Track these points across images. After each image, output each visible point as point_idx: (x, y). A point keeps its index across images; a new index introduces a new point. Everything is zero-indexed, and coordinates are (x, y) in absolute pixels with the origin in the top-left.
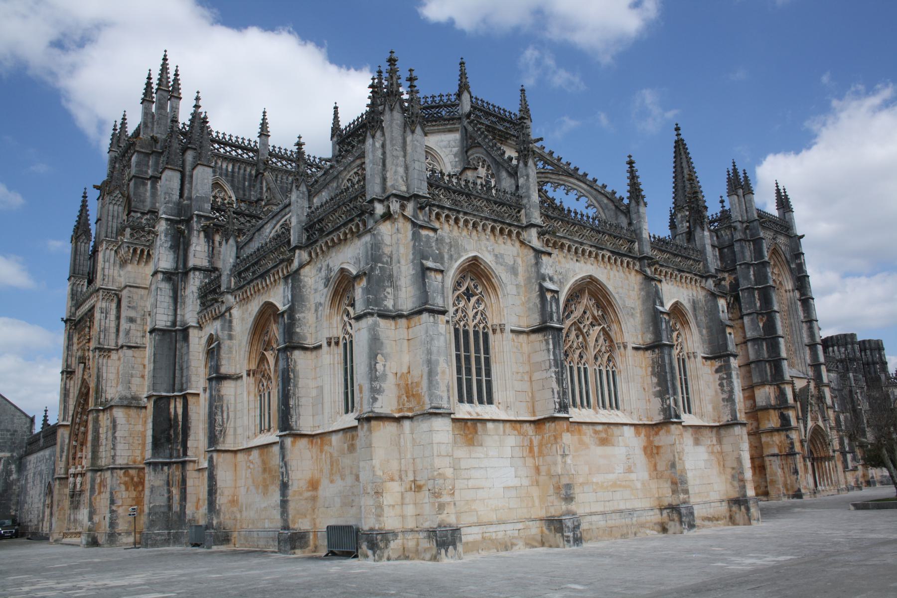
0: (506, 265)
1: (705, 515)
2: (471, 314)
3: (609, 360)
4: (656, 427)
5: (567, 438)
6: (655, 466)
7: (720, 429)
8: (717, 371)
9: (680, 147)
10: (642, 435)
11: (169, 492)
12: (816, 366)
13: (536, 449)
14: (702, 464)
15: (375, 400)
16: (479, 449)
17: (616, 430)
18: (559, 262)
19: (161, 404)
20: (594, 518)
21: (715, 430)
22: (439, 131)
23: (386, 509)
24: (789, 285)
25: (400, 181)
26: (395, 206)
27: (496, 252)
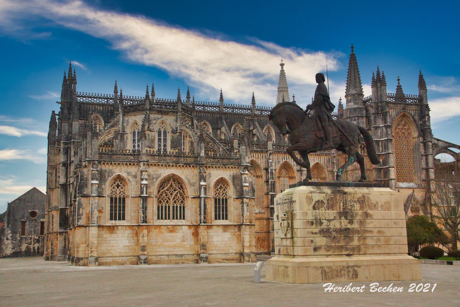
0: (132, 175)
2: (118, 192)
3: (182, 202)
4: (197, 227)
5: (145, 231)
6: (198, 240)
7: (239, 226)
10: (193, 229)
11: (65, 242)
14: (227, 240)
15: (78, 221)
16: (114, 234)
17: (178, 227)
19: (62, 211)
20: (162, 257)
22: (140, 114)
23: (80, 252)
24: (415, 134)
26: (87, 163)
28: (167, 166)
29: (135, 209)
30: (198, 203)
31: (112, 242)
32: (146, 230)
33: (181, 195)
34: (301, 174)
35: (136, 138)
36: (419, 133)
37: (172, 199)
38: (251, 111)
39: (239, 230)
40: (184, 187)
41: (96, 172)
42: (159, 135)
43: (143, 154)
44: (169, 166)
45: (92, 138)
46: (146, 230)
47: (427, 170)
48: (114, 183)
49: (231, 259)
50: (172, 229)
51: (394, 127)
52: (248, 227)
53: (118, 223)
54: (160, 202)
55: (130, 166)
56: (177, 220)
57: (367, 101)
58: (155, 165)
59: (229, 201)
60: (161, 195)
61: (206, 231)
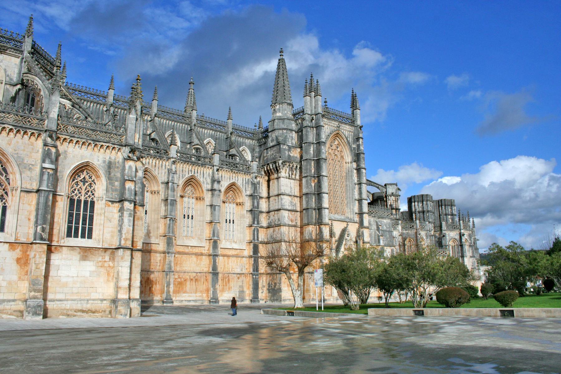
1: (80, 308)
6: (27, 272)
8: (119, 211)
12: (361, 214)
14: (88, 274)
21: (109, 252)
24: (348, 157)
34: (213, 194)
36: (352, 158)
39: (112, 259)
40: (9, 170)
47: (360, 201)
49: (93, 310)
51: (328, 145)
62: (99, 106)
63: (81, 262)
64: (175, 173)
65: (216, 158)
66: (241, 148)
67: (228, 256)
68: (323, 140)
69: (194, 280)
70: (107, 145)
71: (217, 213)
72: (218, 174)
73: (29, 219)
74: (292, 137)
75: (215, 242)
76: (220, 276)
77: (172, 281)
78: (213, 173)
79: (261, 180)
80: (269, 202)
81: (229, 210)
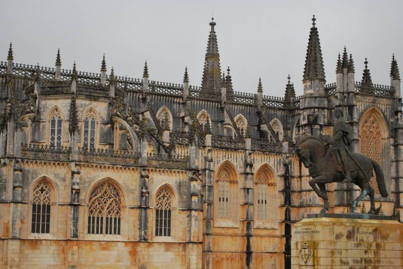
0: (60, 178)
2: (42, 198)
3: (117, 213)
4: (135, 244)
5: (75, 248)
6: (135, 261)
7: (185, 244)
8: (188, 217)
9: (314, 32)
10: (130, 246)
13: (66, 251)
16: (37, 251)
17: (113, 244)
18: (90, 173)
21: (182, 245)
22: (62, 99)
24: (385, 134)
25: (11, 151)
27: (56, 173)
28: (102, 167)
29: (62, 220)
30: (140, 216)
31: (34, 259)
32: (77, 247)
33: (116, 205)
34: (246, 178)
35: (56, 128)
37: (106, 208)
38: (183, 92)
39: (184, 249)
41: (19, 173)
42: (86, 126)
43: (75, 153)
44: (105, 167)
45: (16, 128)
46: (77, 247)
48: (38, 187)
50: (106, 246)
51: (361, 124)
52: (195, 246)
53: (42, 236)
54: (92, 212)
55: (58, 167)
56: (111, 235)
57: (330, 89)
58: (88, 166)
59: (173, 214)
60: (93, 203)
61: (146, 250)
62: (135, 94)
63: (166, 252)
64: (211, 161)
65: (248, 142)
66: (273, 120)
67: (261, 236)
68: (355, 120)
69: (230, 259)
70: (178, 170)
71: (250, 195)
72: (250, 157)
73: (134, 226)
74: (324, 115)
75: (249, 224)
76: (254, 255)
77: (211, 260)
78: (246, 157)
79: (293, 159)
80: (301, 181)
81: (262, 191)
